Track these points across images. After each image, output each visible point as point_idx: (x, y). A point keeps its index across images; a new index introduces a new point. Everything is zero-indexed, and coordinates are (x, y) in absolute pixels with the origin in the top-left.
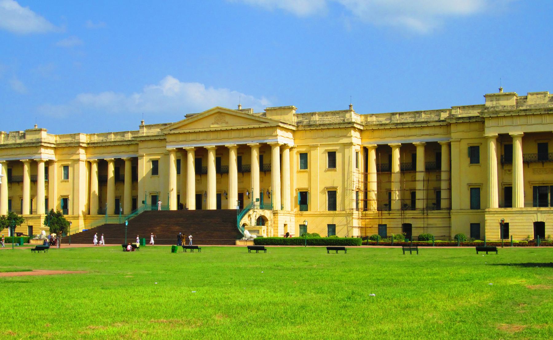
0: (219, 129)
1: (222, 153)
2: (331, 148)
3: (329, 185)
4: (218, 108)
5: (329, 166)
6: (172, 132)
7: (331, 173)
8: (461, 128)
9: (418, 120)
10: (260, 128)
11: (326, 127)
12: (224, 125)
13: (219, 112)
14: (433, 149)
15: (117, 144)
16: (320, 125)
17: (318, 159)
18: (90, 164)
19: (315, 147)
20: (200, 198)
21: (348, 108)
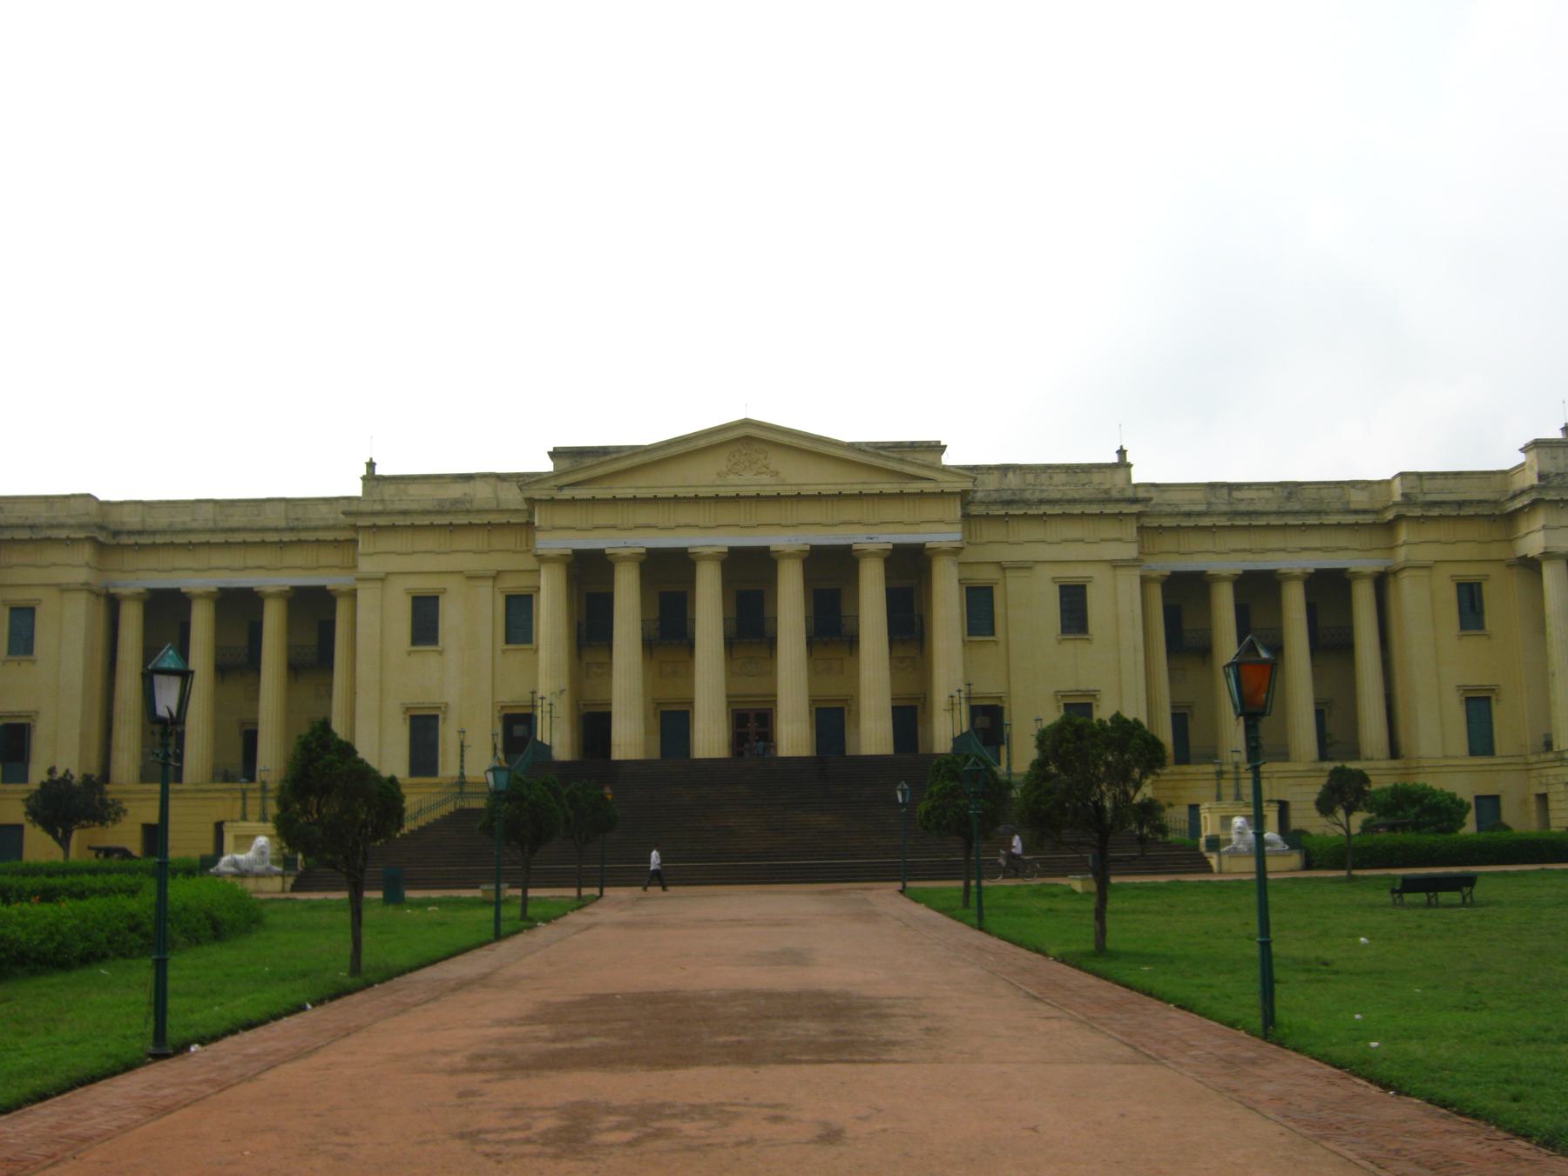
0: (855, 489)
1: (750, 574)
2: (1073, 574)
3: (1068, 685)
4: (746, 423)
5: (1066, 629)
6: (567, 494)
7: (1074, 648)
8: (1431, 532)
9: (1289, 507)
10: (902, 495)
11: (1057, 510)
12: (765, 479)
13: (748, 440)
14: (1328, 589)
15: (239, 537)
16: (1041, 502)
17: (1030, 608)
18: (113, 604)
19: (1025, 567)
20: (674, 723)
21: (1114, 459)
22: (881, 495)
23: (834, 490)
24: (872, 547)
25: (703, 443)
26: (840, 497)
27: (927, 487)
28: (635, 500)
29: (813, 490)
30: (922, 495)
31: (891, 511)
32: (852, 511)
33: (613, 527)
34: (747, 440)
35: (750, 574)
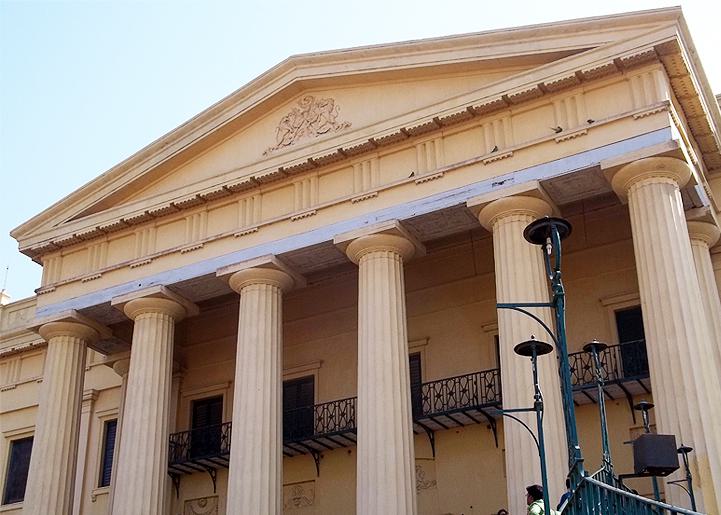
4: (294, 63)
10: (544, 91)
22: (508, 103)
23: (424, 118)
24: (500, 195)
25: (235, 112)
26: (439, 125)
27: (585, 64)
28: (150, 218)
29: (392, 128)
30: (581, 79)
31: (533, 125)
32: (464, 146)
33: (125, 266)
34: (297, 88)
35: (318, 287)
